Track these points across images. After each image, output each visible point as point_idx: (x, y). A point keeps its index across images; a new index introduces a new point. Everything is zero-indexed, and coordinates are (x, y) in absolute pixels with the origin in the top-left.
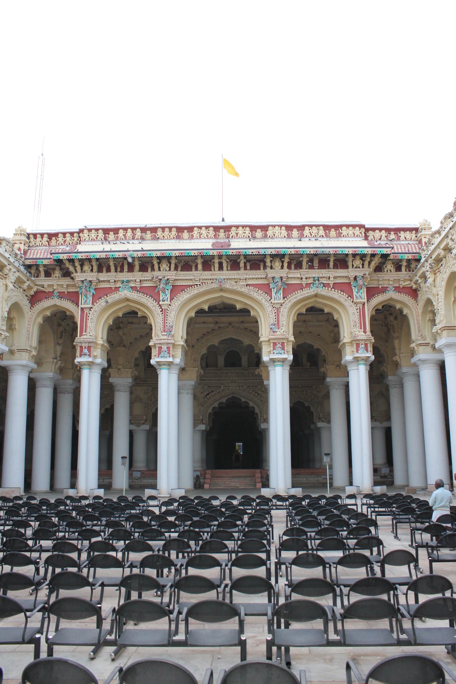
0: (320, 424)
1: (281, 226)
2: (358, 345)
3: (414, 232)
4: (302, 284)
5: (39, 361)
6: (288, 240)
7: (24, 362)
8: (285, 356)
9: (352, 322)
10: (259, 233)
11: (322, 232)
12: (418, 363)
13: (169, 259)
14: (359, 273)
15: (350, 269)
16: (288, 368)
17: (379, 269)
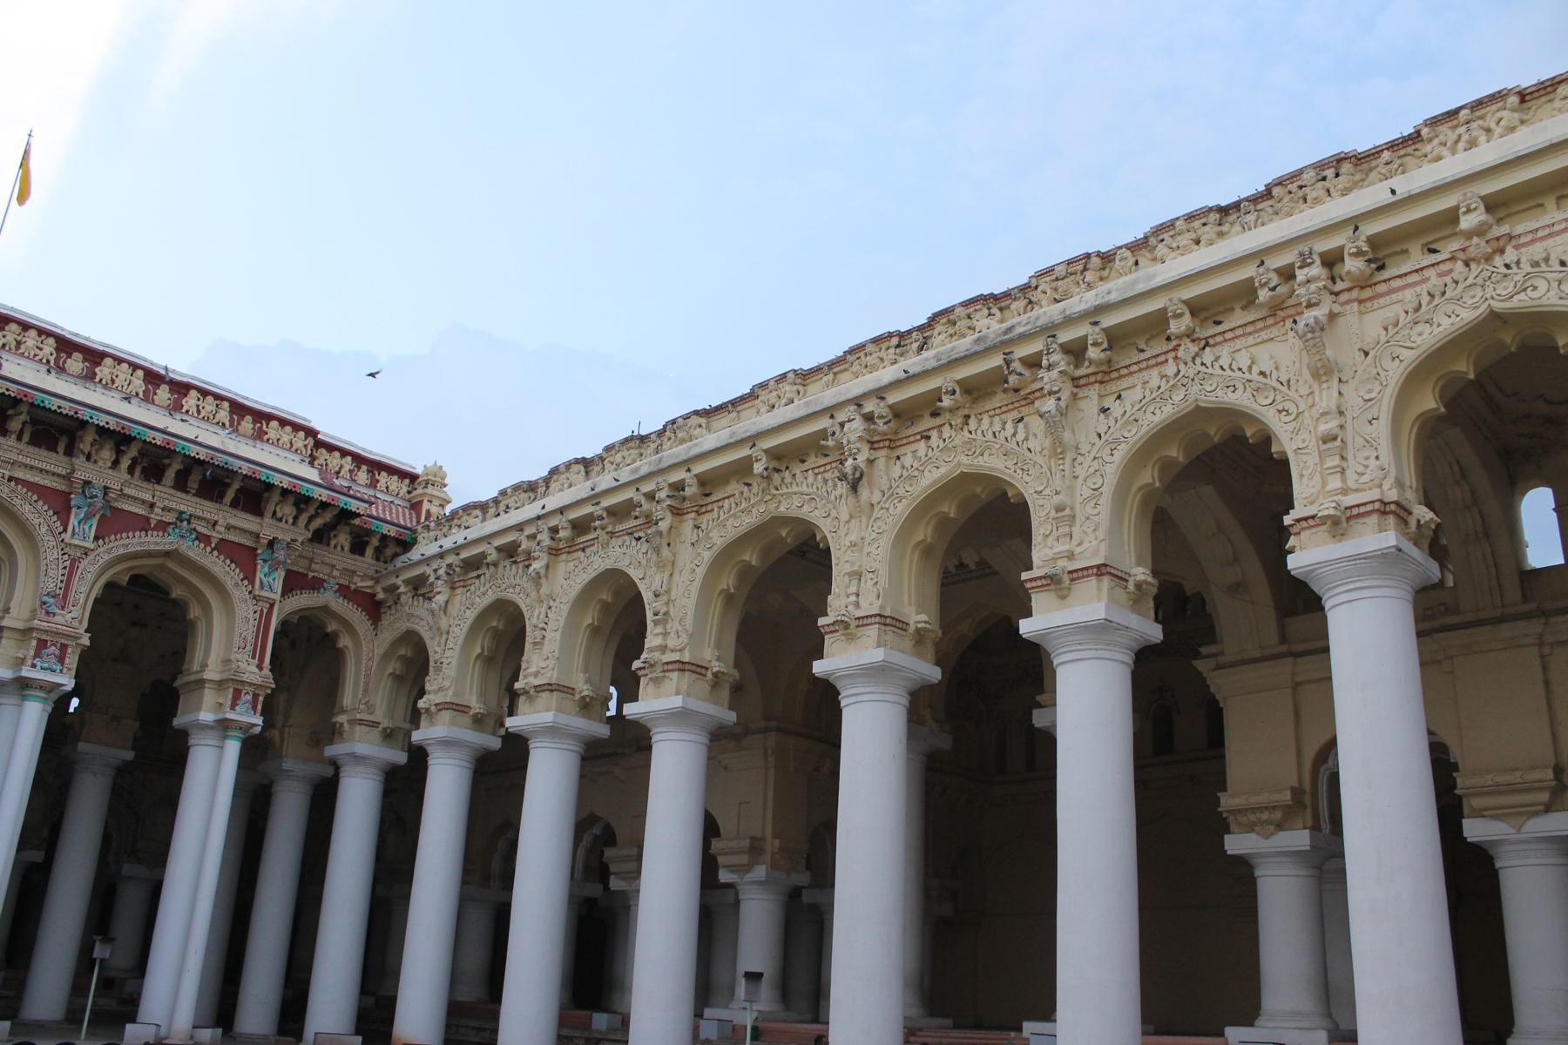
1: (135, 367)
2: (237, 694)
3: (407, 481)
4: (148, 519)
6: (143, 404)
9: (236, 638)
10: (75, 364)
11: (223, 415)
14: (283, 533)
15: (267, 520)
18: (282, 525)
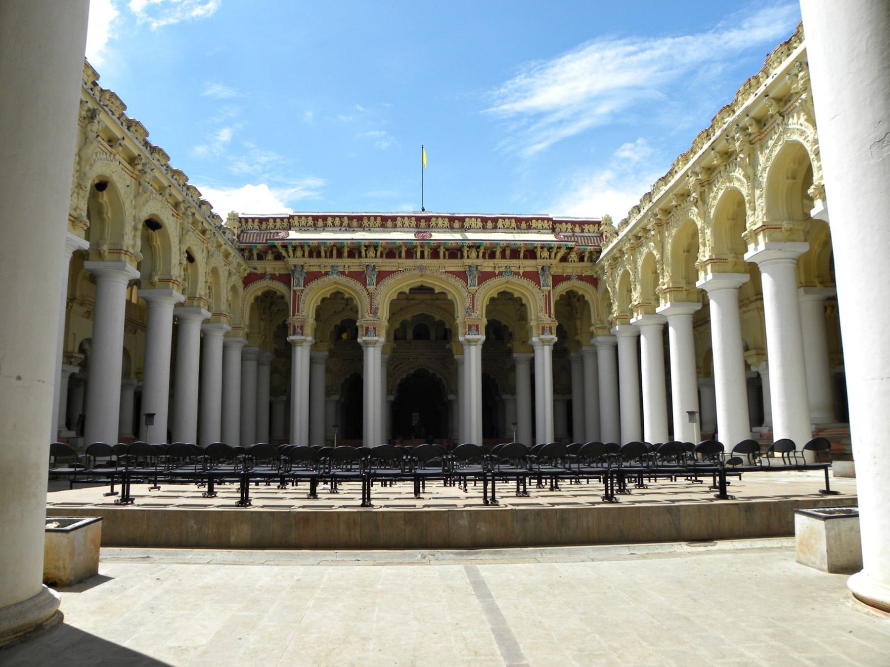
0: (505, 396)
1: (477, 218)
2: (543, 328)
5: (248, 336)
7: (241, 339)
10: (457, 224)
11: (514, 224)
12: (597, 344)
13: (376, 247)
16: (480, 347)
17: (564, 259)
18: (545, 260)
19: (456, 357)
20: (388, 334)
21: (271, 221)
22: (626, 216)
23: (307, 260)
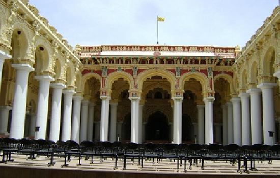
0: (193, 123)
2: (209, 94)
5: (84, 96)
8: (180, 98)
11: (196, 49)
17: (218, 64)
19: (172, 106)
20: (142, 95)
21: (94, 48)
22: (245, 46)
23: (108, 64)
